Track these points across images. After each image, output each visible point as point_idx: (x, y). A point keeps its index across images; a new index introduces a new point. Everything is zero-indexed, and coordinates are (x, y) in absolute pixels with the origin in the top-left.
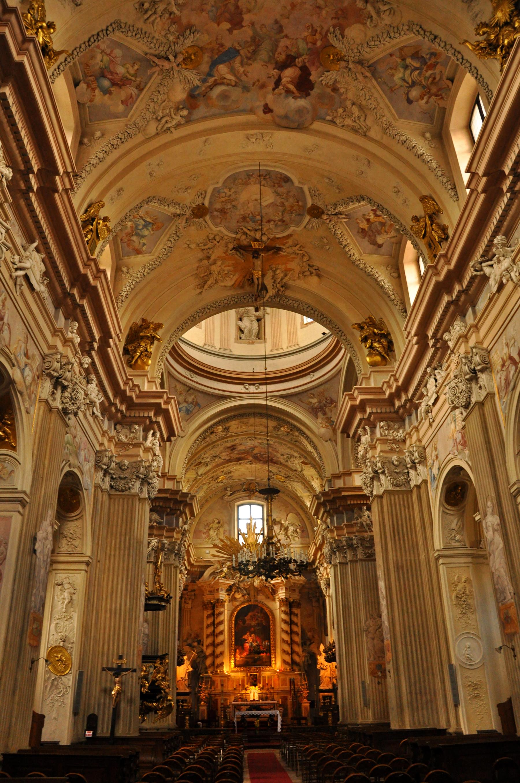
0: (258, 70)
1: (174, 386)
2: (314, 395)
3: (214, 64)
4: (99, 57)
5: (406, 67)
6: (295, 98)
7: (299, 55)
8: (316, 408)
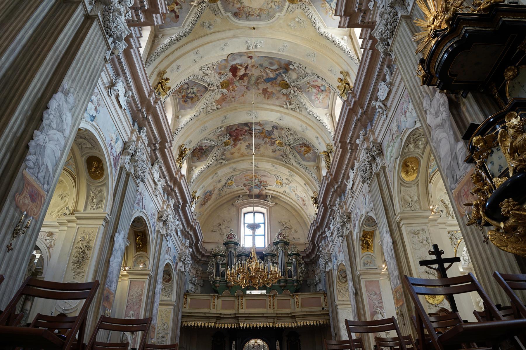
0: (255, 73)
3: (275, 78)
4: (321, 98)
5: (193, 93)
6: (237, 64)
7: (238, 80)
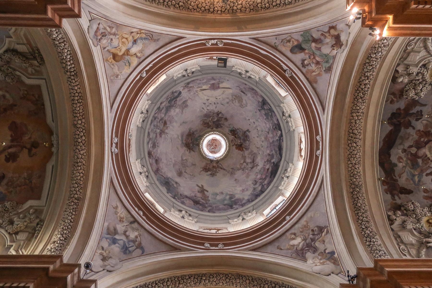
1: (115, 205)
2: (295, 234)
8: (302, 249)
